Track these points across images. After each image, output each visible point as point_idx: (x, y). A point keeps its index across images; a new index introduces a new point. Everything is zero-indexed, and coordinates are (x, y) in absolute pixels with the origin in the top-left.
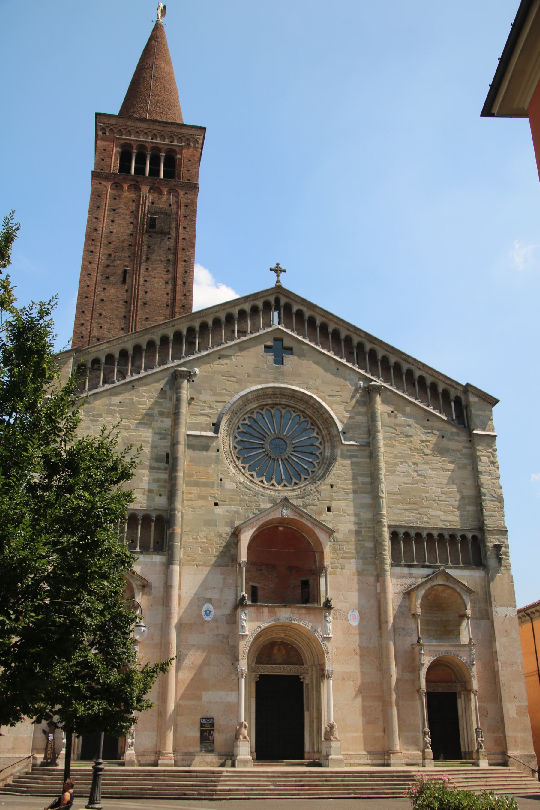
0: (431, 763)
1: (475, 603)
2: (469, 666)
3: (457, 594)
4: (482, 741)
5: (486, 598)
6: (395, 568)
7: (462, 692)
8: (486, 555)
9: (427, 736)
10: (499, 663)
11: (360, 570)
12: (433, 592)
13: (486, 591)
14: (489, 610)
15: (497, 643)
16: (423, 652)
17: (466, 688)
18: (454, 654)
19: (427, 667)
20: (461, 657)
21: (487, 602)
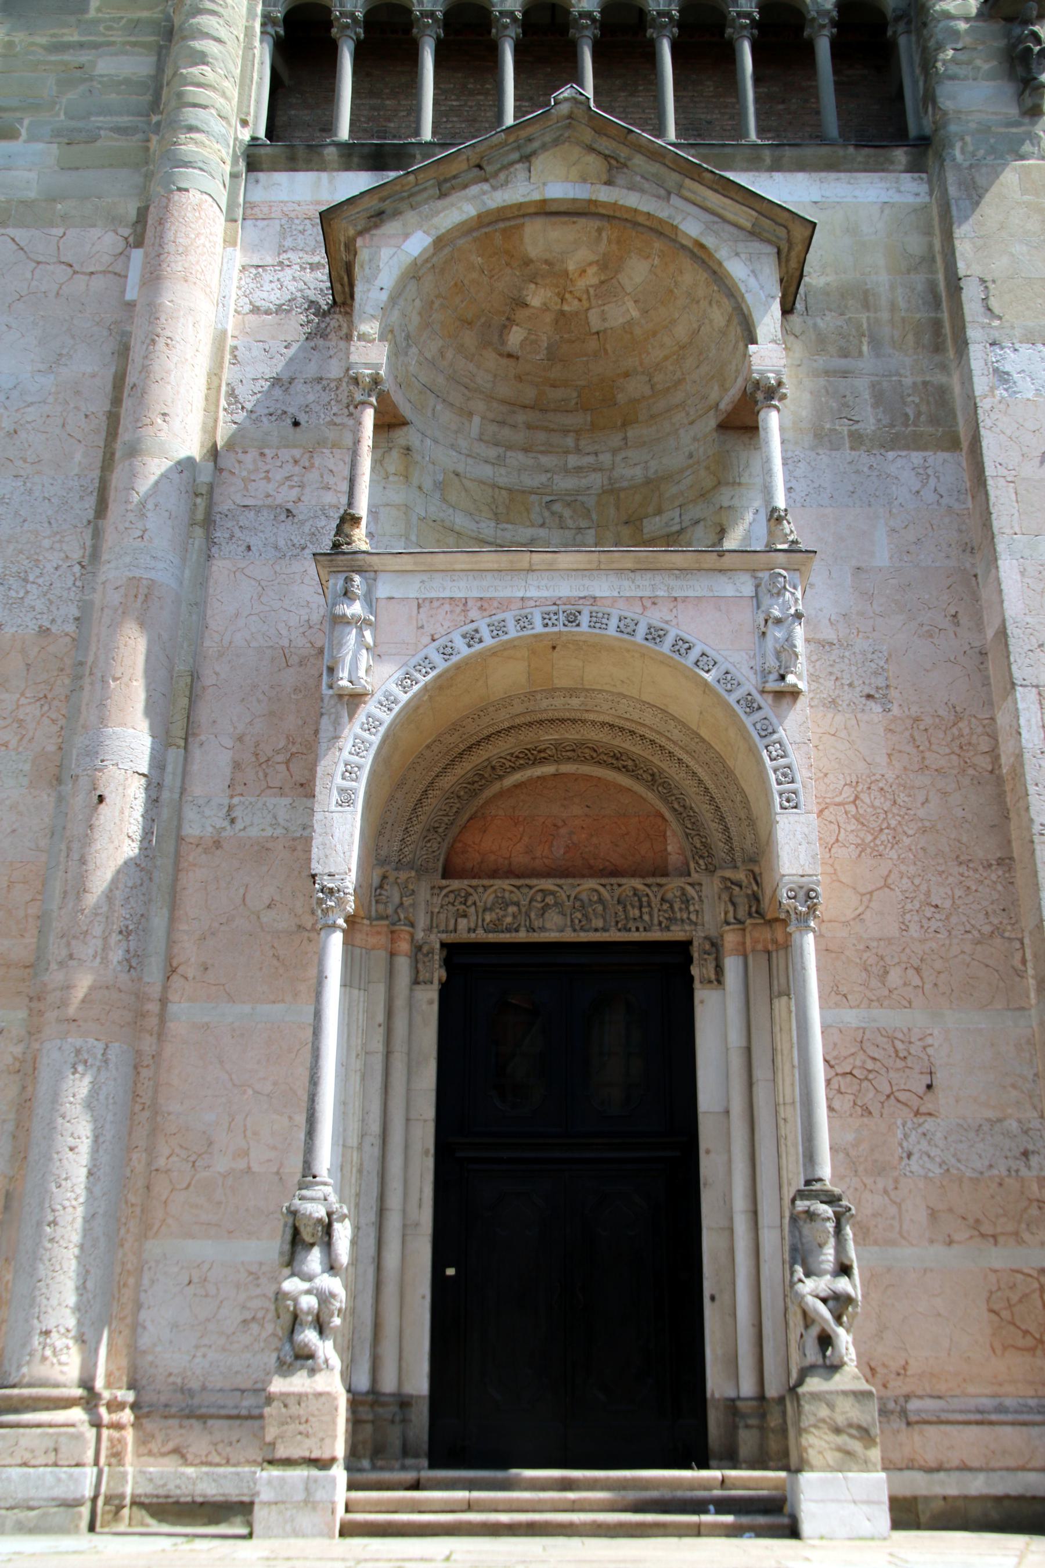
0: (309, 1503)
1: (845, 355)
2: (752, 707)
3: (691, 276)
4: (839, 1303)
5: (937, 325)
6: (282, 177)
7: (730, 939)
8: (927, 64)
9: (314, 1259)
10: (1026, 701)
11: (32, 195)
12: (537, 297)
13: (932, 287)
14: (957, 389)
15: (1008, 569)
16: (355, 609)
17: (756, 898)
18: (627, 627)
19: (387, 718)
20: (682, 646)
21: (938, 348)
